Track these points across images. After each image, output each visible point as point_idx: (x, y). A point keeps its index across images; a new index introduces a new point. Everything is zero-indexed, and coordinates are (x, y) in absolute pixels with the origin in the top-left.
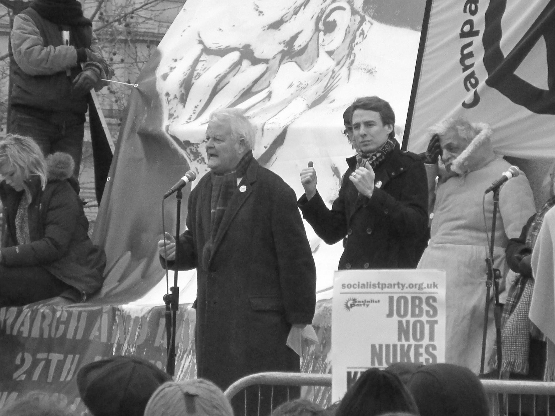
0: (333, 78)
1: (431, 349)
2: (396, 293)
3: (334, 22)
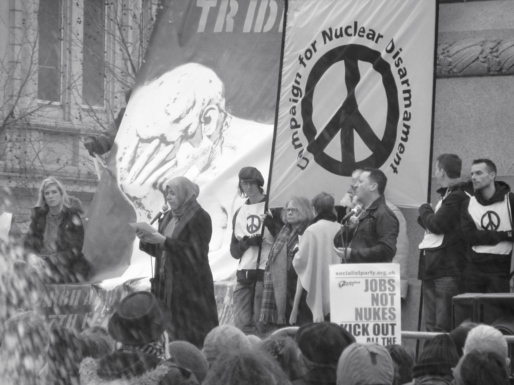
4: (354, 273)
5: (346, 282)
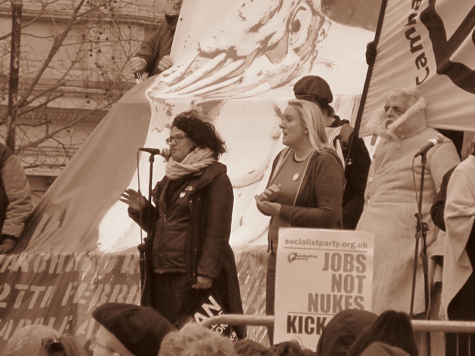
1: (359, 300)
2: (332, 249)
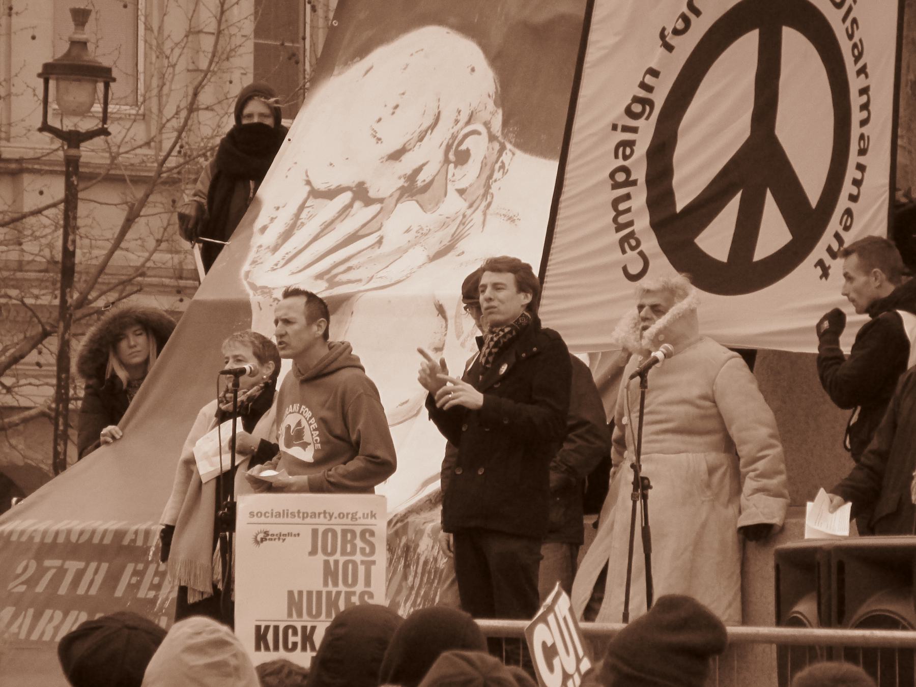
0: (464, 224)
3: (468, 151)
4: (287, 513)
5: (270, 533)
